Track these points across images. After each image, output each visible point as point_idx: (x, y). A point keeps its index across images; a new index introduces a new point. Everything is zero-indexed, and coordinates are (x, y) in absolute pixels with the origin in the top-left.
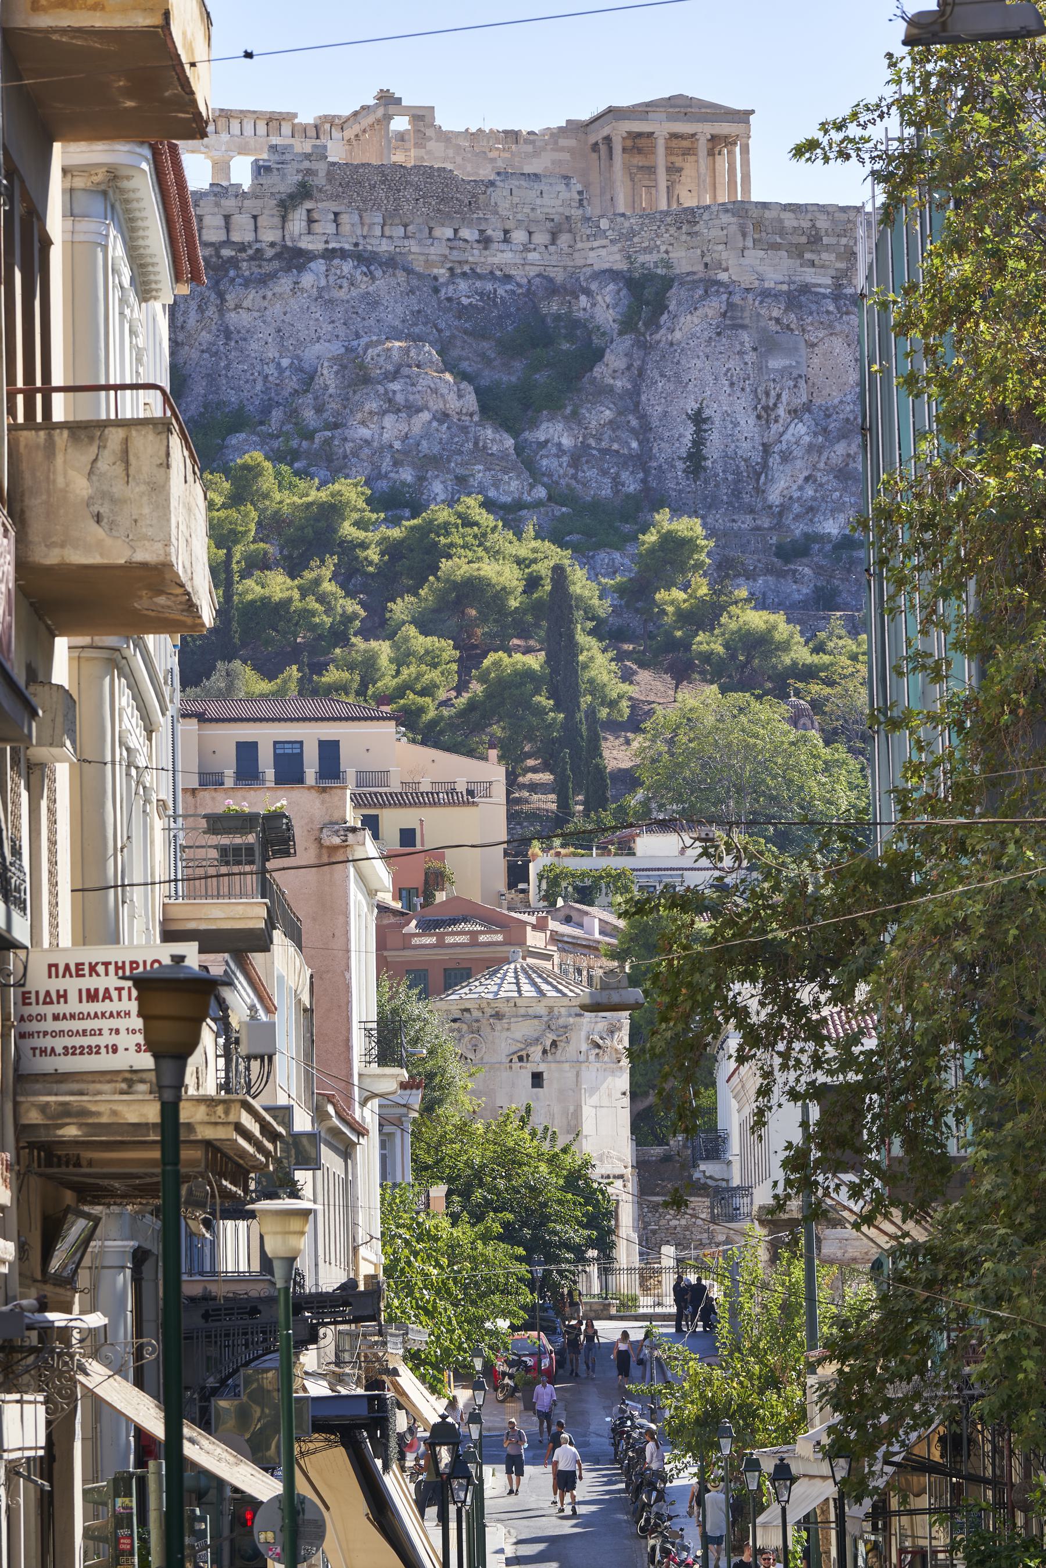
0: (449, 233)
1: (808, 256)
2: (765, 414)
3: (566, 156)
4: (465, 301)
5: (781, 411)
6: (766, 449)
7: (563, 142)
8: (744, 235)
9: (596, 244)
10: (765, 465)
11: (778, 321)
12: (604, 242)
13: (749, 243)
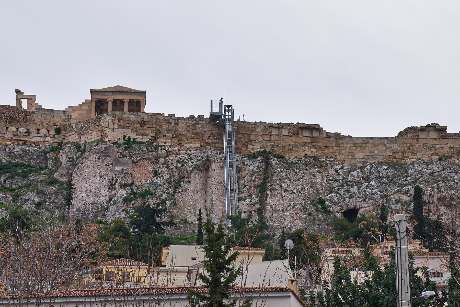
0: (14, 129)
1: (140, 131)
2: (111, 187)
3: (85, 112)
4: (16, 153)
5: (117, 186)
6: (110, 199)
7: (83, 107)
8: (114, 123)
9: (71, 134)
10: (108, 206)
11: (121, 153)
12: (74, 132)
13: (116, 127)
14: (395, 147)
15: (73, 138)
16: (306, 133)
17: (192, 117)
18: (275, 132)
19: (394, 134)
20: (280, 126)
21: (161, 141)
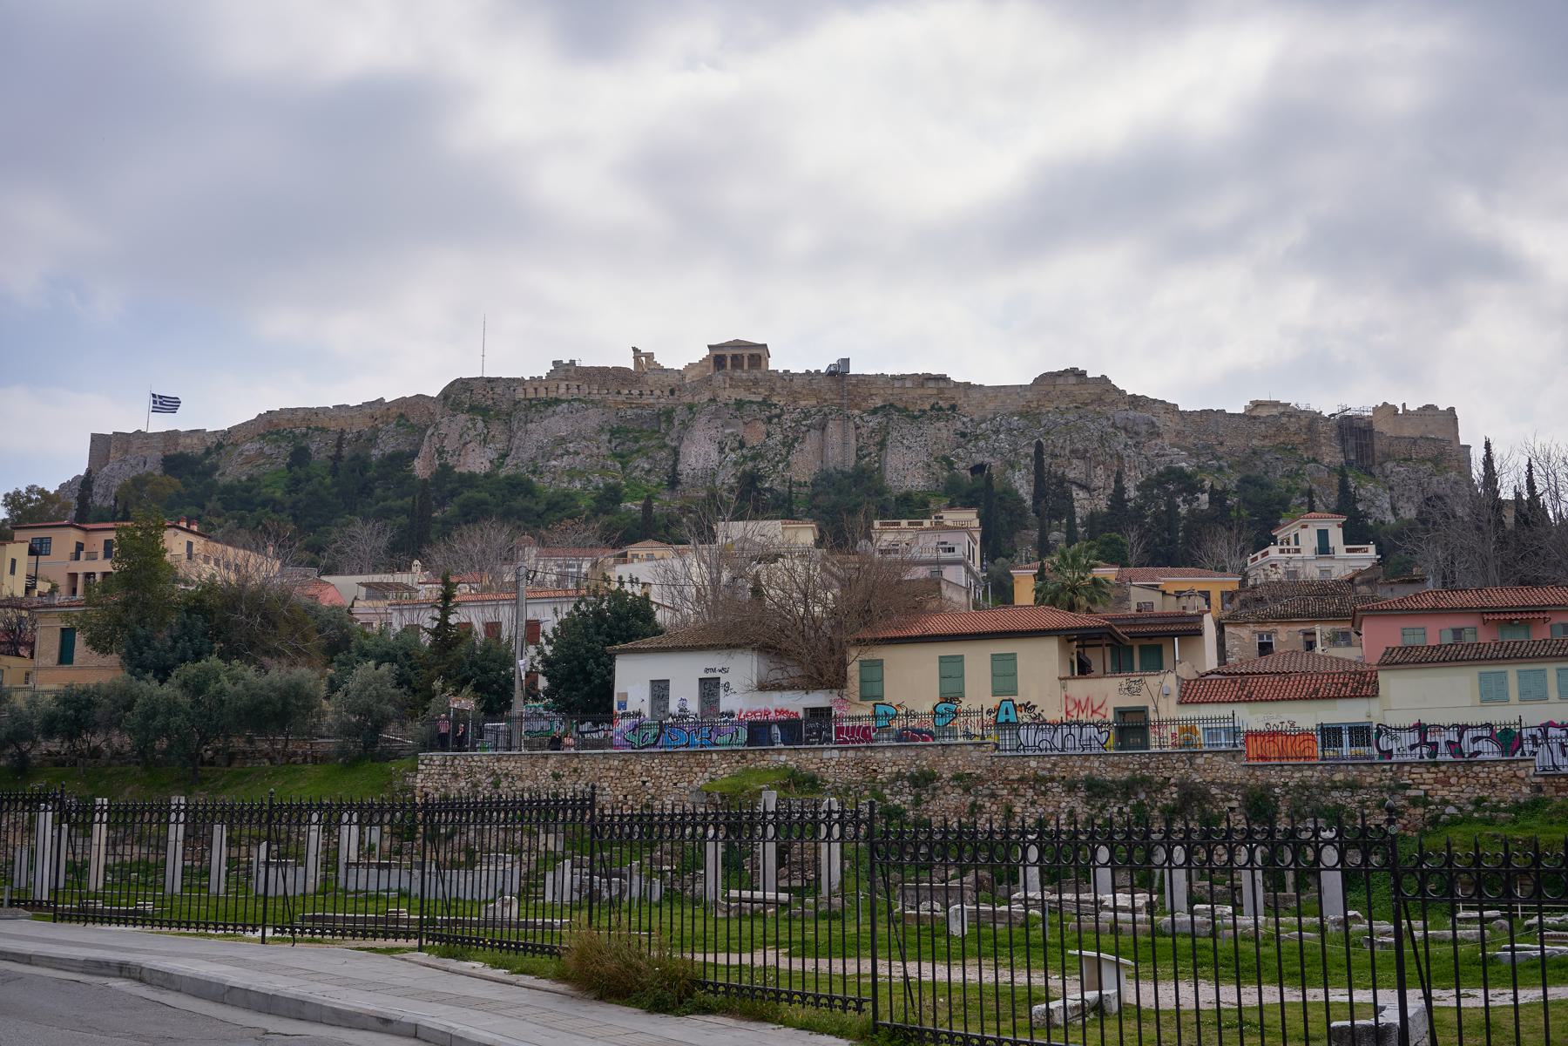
14: (1029, 395)
15: (688, 399)
16: (931, 384)
17: (808, 372)
18: (897, 384)
19: (1029, 382)
20: (903, 378)
21: (775, 400)
